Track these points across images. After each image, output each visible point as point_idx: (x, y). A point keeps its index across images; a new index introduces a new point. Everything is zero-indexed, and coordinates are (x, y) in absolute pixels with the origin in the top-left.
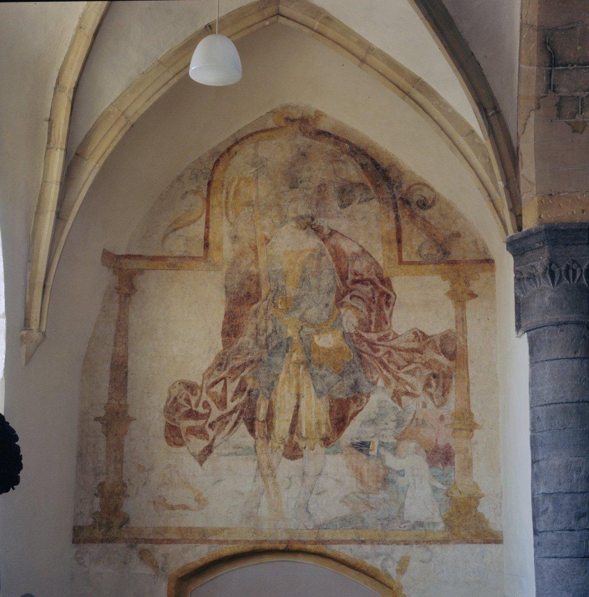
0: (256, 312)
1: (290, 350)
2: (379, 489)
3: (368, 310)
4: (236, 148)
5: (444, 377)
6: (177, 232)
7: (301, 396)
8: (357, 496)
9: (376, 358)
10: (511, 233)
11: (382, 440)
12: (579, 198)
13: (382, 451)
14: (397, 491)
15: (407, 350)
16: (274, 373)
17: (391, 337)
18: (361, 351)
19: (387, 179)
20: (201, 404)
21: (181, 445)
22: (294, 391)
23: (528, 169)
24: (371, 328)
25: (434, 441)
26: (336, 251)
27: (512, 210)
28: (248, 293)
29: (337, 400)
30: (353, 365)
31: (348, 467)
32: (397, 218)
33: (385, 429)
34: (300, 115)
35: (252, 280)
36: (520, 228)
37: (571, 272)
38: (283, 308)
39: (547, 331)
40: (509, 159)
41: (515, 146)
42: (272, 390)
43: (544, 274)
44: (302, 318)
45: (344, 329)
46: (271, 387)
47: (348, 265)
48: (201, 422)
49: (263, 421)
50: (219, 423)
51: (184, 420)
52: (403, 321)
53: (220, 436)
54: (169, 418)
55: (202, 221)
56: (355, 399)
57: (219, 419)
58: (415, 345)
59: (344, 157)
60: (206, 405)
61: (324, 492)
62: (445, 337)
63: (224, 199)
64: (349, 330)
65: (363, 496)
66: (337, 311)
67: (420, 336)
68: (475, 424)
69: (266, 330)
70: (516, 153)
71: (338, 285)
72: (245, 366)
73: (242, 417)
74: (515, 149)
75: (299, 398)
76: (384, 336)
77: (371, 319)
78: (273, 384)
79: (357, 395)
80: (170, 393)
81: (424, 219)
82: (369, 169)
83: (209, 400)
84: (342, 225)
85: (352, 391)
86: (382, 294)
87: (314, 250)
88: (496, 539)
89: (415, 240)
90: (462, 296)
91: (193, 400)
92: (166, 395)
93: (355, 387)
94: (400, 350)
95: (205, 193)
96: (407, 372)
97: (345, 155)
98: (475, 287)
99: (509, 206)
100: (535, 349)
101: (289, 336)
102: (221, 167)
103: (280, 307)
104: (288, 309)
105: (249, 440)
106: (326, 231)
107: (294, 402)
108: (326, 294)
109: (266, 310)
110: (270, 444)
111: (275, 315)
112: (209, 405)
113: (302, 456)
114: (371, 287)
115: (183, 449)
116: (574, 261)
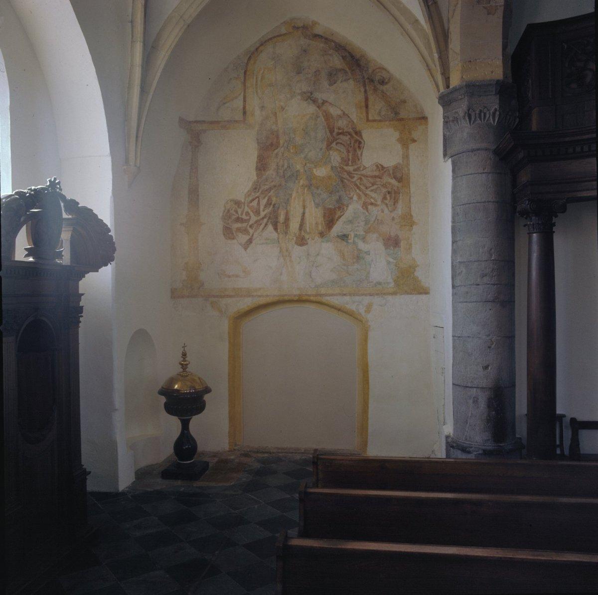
0: (277, 154)
1: (298, 178)
2: (354, 263)
4: (261, 48)
5: (395, 193)
6: (226, 105)
8: (341, 267)
9: (352, 182)
10: (442, 90)
11: (356, 233)
12: (489, 63)
13: (356, 239)
14: (365, 264)
15: (372, 177)
17: (361, 169)
19: (359, 65)
20: (244, 214)
21: (233, 239)
22: (301, 203)
23: (455, 44)
25: (388, 233)
26: (326, 114)
27: (443, 74)
28: (272, 143)
29: (328, 209)
31: (335, 250)
32: (365, 91)
33: (358, 226)
34: (302, 25)
35: (273, 134)
36: (448, 87)
37: (482, 114)
39: (465, 156)
40: (442, 36)
41: (446, 28)
43: (464, 116)
44: (305, 157)
46: (287, 202)
47: (334, 124)
48: (245, 225)
49: (283, 223)
50: (255, 225)
51: (234, 223)
52: (369, 158)
53: (257, 233)
54: (225, 223)
55: (241, 97)
56: (339, 208)
57: (256, 222)
58: (377, 173)
59: (331, 52)
60: (247, 214)
61: (321, 265)
62: (396, 168)
63: (254, 83)
65: (345, 267)
66: (328, 153)
67: (380, 168)
68: (414, 222)
69: (283, 166)
70: (447, 33)
72: (270, 189)
73: (270, 221)
74: (446, 31)
75: (304, 208)
78: (288, 199)
79: (341, 206)
80: (225, 207)
81: (383, 92)
82: (347, 59)
83: (249, 211)
84: (331, 98)
86: (356, 141)
87: (313, 114)
88: (425, 292)
89: (377, 106)
90: (406, 141)
91: (240, 211)
92: (223, 209)
93: (340, 200)
94: (367, 177)
95: (242, 79)
96: (372, 190)
97: (332, 51)
98: (415, 135)
99: (441, 71)
100: (456, 168)
102: (252, 62)
104: (296, 152)
105: (275, 235)
106: (320, 101)
107: (301, 211)
109: (283, 154)
110: (287, 237)
112: (249, 214)
113: (307, 244)
114: (349, 136)
115: (235, 241)
116: (486, 107)
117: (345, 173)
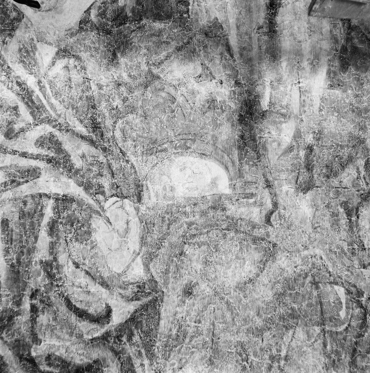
1: (302, 153)
3: (58, 267)
7: (265, 30)
9: (49, 121)
16: (345, 91)
18: (92, 143)
24: (54, 209)
29: (169, 16)
30: (117, 102)
38: (329, 288)
42: (344, 49)
44: (270, 252)
45: (137, 210)
64: (122, 207)
66: (156, 269)
71: (146, 362)
76: (19, 184)
77: (48, 239)
85: (125, 36)
101: (309, 195)
103: (341, 291)
108: (191, 330)
111: (356, 263)
114: (37, 352)
117: (78, 163)
